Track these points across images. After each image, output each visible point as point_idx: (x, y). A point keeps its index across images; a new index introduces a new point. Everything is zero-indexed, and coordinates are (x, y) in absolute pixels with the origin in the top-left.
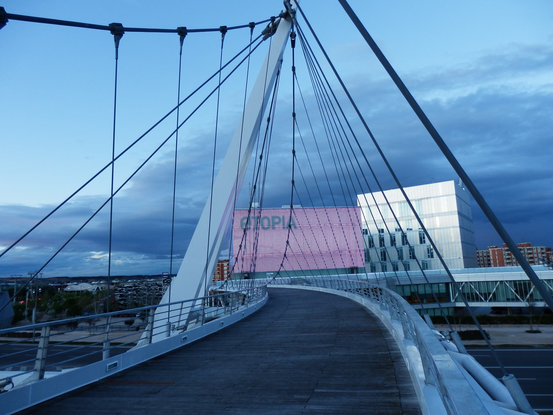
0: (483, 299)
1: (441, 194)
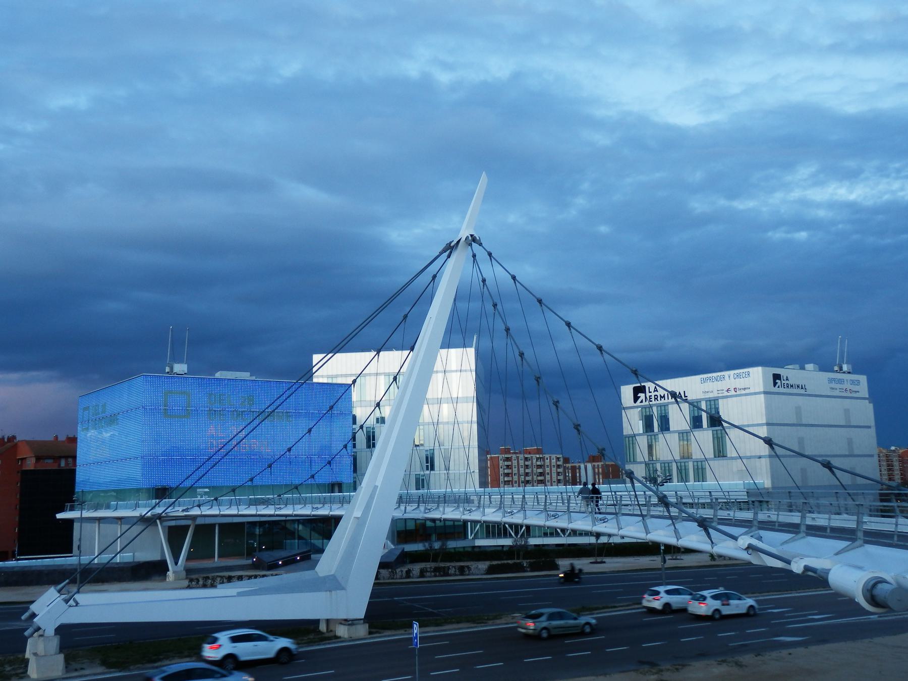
0: (513, 534)
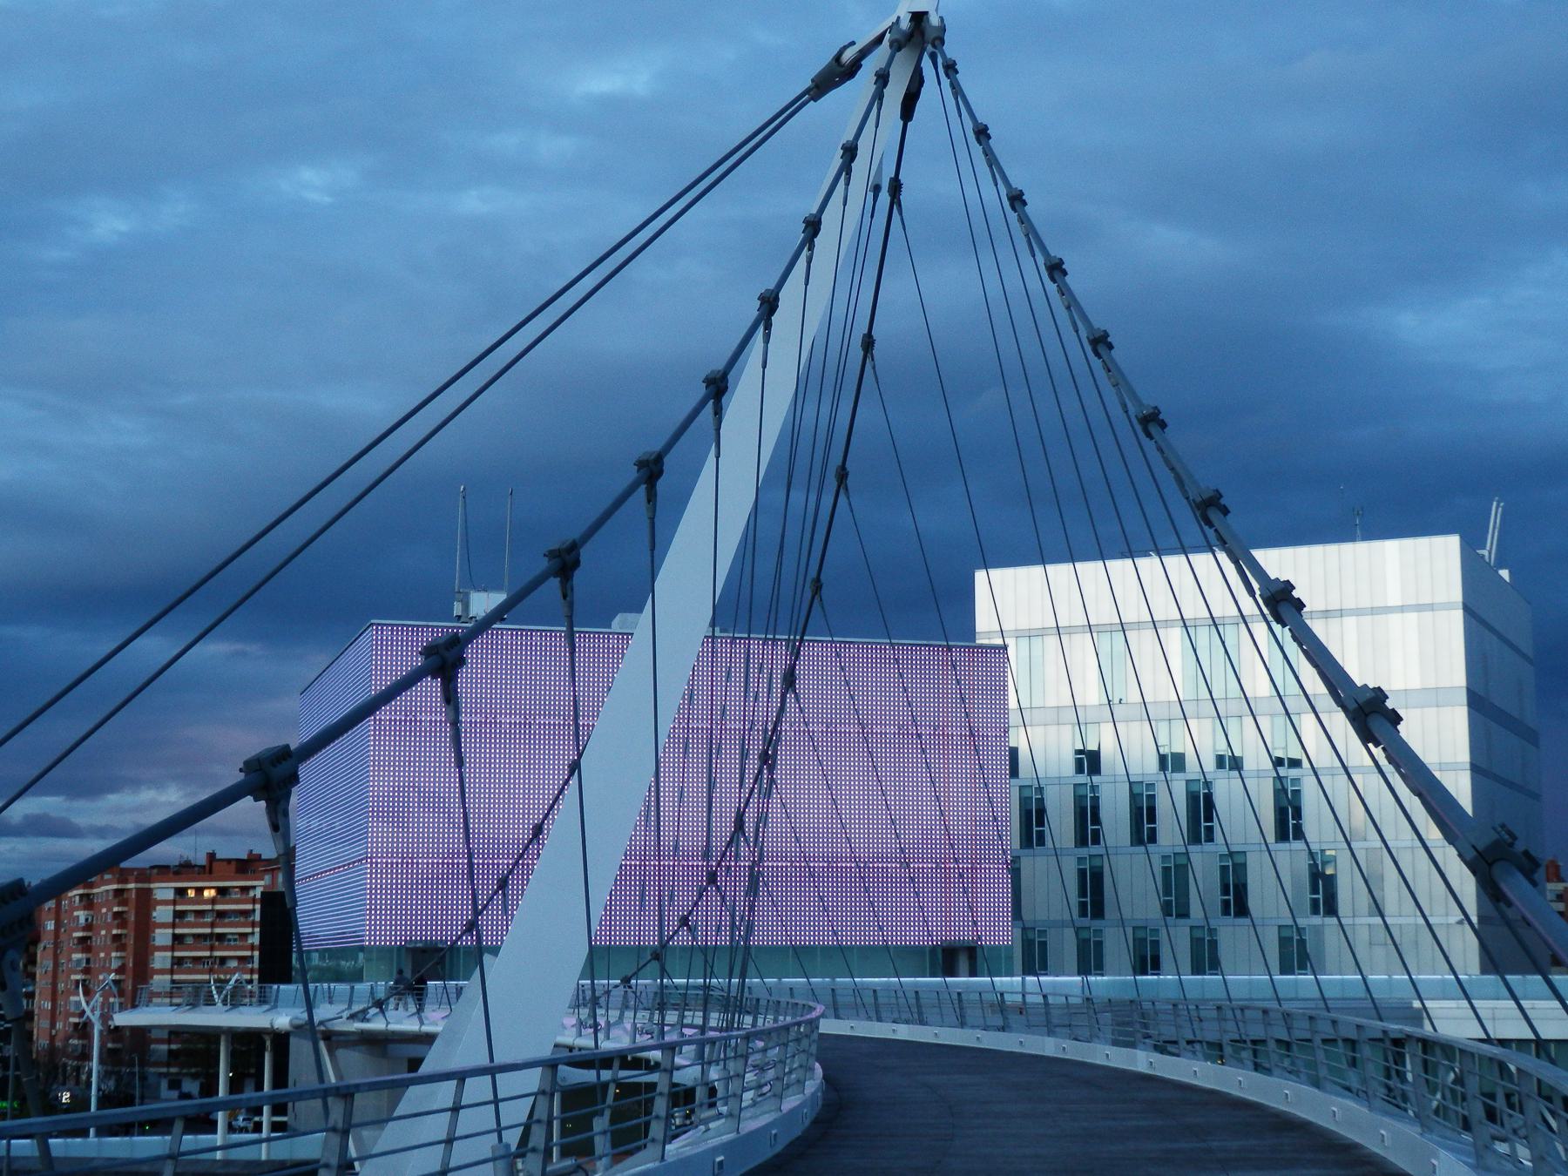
1: (1394, 600)
